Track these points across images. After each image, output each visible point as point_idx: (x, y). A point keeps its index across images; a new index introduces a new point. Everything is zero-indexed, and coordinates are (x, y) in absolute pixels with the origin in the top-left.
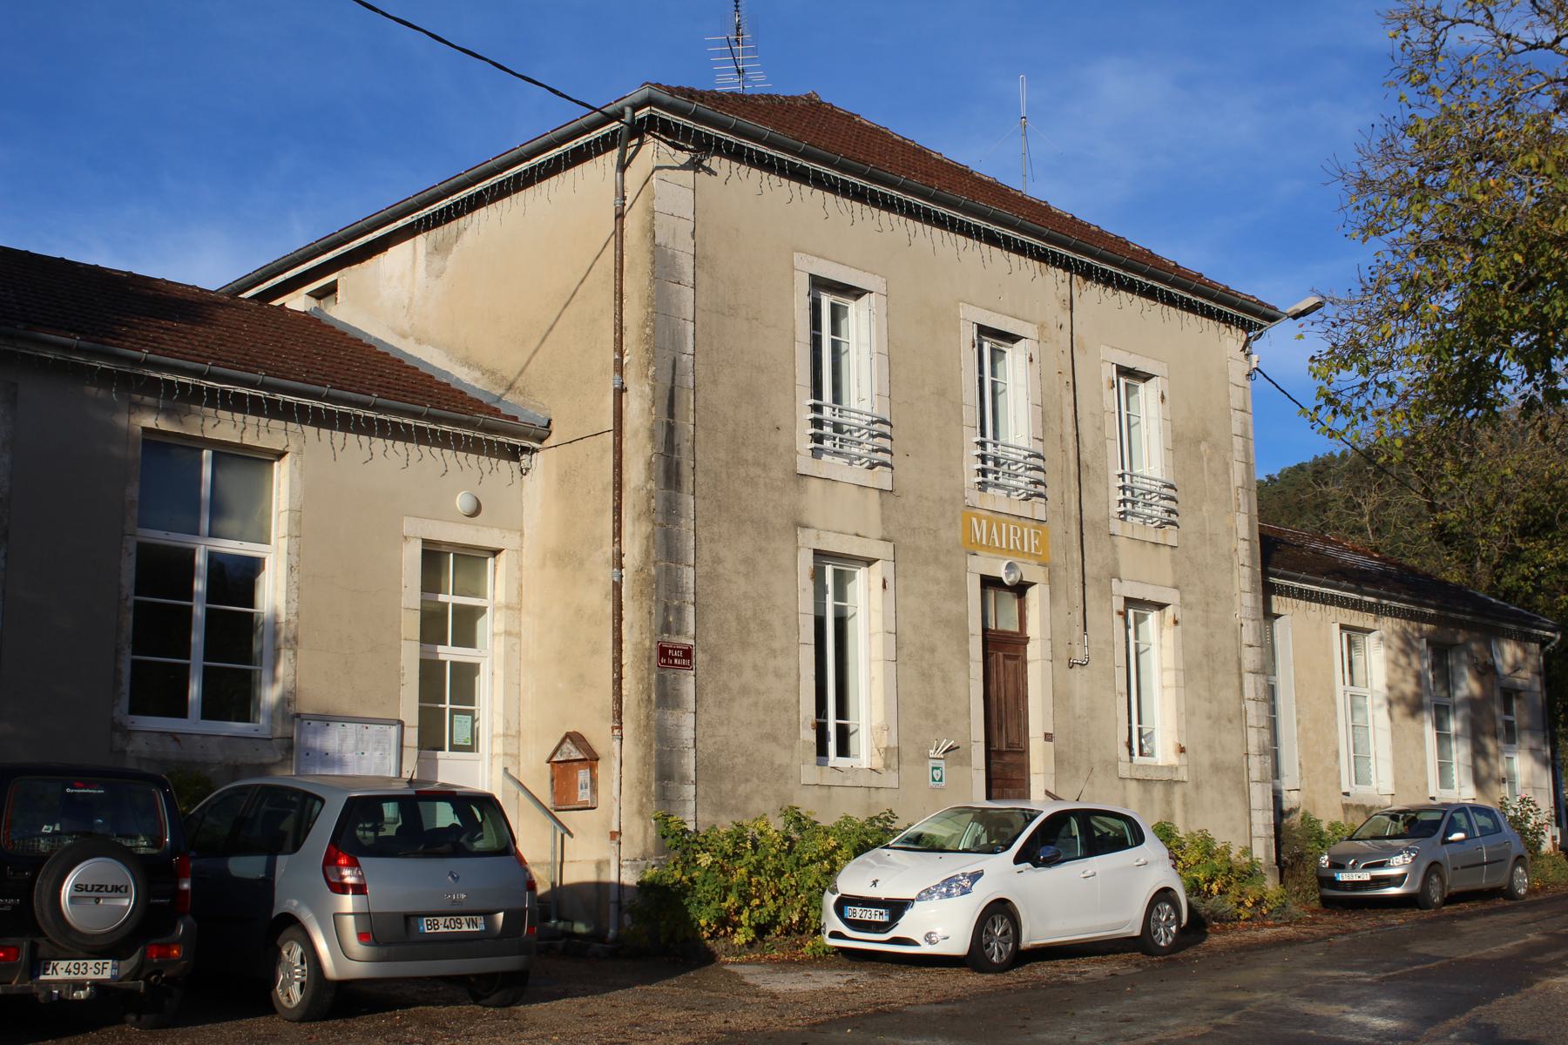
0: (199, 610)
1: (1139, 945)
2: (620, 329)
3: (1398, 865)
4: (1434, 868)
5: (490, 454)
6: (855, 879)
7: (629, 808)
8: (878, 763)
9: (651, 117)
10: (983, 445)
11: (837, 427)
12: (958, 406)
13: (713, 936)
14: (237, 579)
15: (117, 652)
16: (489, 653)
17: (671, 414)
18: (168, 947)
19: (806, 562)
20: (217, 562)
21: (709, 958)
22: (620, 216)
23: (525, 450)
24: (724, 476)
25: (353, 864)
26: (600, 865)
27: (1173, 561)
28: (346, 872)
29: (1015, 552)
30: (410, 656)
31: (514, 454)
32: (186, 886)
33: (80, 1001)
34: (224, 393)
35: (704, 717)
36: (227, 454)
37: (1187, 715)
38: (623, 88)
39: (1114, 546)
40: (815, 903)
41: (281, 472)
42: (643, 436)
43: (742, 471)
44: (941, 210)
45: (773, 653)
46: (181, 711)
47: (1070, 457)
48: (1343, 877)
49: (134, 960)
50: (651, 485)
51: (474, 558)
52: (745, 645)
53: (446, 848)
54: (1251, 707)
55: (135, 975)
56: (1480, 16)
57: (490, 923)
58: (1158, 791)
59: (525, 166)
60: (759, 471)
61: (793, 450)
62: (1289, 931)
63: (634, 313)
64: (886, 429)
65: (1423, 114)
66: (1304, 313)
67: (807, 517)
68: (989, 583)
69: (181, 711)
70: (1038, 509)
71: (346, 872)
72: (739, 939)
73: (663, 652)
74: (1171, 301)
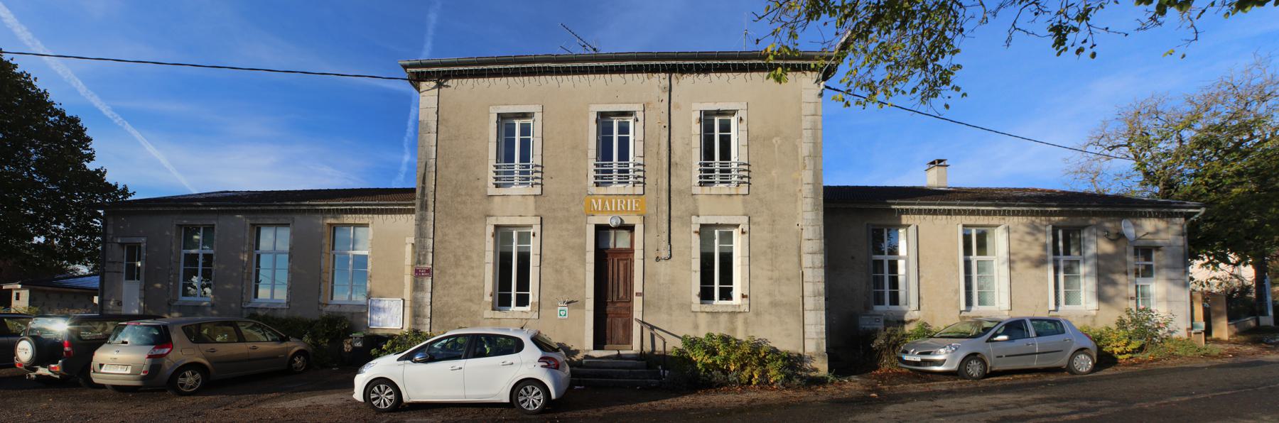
27: (745, 202)
45: (472, 268)
48: (906, 358)
52: (457, 265)
61: (486, 186)
73: (417, 271)
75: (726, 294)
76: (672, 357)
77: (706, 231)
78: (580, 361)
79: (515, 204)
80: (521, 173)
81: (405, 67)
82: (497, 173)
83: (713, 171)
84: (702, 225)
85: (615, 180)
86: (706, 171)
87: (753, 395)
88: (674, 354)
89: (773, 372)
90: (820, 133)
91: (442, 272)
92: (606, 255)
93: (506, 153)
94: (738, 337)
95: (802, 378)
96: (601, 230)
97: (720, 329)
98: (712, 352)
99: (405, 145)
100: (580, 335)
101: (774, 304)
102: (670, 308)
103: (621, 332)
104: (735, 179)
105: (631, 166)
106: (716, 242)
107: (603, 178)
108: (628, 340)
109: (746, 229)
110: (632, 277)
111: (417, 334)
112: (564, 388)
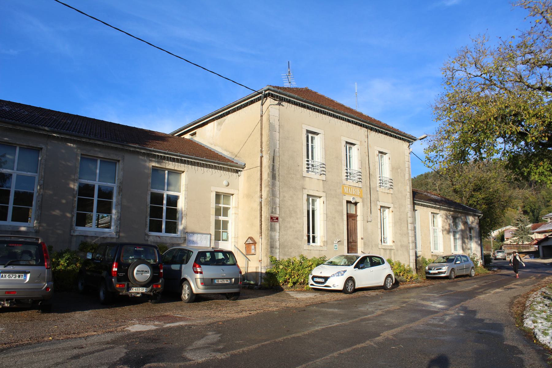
0: (165, 208)
1: (383, 287)
2: (262, 143)
3: (444, 269)
4: (453, 270)
5: (231, 172)
6: (317, 271)
7: (264, 254)
8: (322, 245)
9: (269, 93)
10: (347, 170)
11: (313, 165)
12: (341, 160)
13: (283, 285)
14: (173, 201)
15: (146, 217)
16: (231, 218)
17: (274, 162)
18: (158, 285)
19: (305, 197)
20: (169, 197)
21: (282, 290)
22: (262, 116)
23: (239, 171)
25: (200, 267)
26: (257, 268)
28: (198, 269)
29: (355, 195)
30: (213, 218)
31: (237, 172)
32: (162, 271)
33: (138, 297)
34: (171, 158)
35: (281, 234)
36: (171, 172)
37: (395, 234)
38: (262, 86)
39: (378, 194)
40: (307, 277)
41: (183, 176)
42: (267, 167)
44: (337, 114)
45: (297, 219)
46: (161, 231)
47: (367, 173)
48: (431, 272)
49: (150, 288)
50: (269, 179)
51: (227, 196)
53: (221, 263)
54: (410, 232)
55: (151, 291)
56: (463, 69)
57: (231, 281)
58: (388, 252)
59: (240, 105)
61: (302, 171)
62: (418, 284)
63: (265, 139)
64: (324, 166)
65: (450, 92)
66: (422, 139)
67: (305, 187)
68: (348, 202)
69: (161, 231)
70: (360, 185)
71: (198, 269)
72: (289, 285)
73: (272, 218)
74: (391, 136)
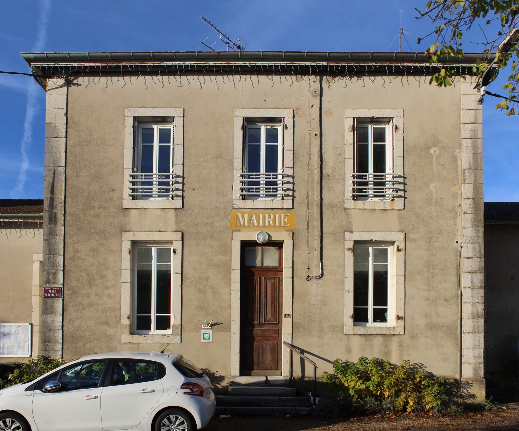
24: (82, 215)
39: (348, 215)
43: (92, 212)
45: (107, 288)
60: (101, 210)
61: (121, 198)
73: (46, 291)
75: (380, 316)
76: (322, 383)
77: (359, 247)
78: (226, 388)
79: (153, 218)
80: (160, 184)
81: (29, 61)
82: (133, 183)
83: (366, 184)
84: (356, 242)
85: (262, 192)
86: (359, 184)
87: (408, 423)
88: (325, 380)
89: (428, 399)
90: (480, 143)
91: (75, 292)
92: (253, 274)
93: (143, 161)
94: (393, 362)
95: (459, 405)
96: (248, 247)
97: (374, 353)
98: (365, 377)
99: (23, 150)
100: (226, 362)
101: (430, 327)
102: (322, 331)
103: (269, 356)
104: (390, 192)
105: (280, 177)
106: (371, 260)
107: (250, 190)
108: (277, 365)
109: (402, 246)
110: (280, 297)
111: (47, 361)
112: (209, 416)
